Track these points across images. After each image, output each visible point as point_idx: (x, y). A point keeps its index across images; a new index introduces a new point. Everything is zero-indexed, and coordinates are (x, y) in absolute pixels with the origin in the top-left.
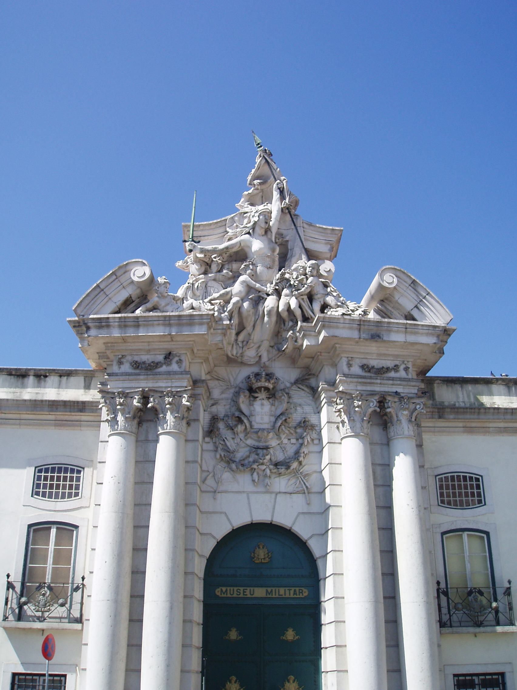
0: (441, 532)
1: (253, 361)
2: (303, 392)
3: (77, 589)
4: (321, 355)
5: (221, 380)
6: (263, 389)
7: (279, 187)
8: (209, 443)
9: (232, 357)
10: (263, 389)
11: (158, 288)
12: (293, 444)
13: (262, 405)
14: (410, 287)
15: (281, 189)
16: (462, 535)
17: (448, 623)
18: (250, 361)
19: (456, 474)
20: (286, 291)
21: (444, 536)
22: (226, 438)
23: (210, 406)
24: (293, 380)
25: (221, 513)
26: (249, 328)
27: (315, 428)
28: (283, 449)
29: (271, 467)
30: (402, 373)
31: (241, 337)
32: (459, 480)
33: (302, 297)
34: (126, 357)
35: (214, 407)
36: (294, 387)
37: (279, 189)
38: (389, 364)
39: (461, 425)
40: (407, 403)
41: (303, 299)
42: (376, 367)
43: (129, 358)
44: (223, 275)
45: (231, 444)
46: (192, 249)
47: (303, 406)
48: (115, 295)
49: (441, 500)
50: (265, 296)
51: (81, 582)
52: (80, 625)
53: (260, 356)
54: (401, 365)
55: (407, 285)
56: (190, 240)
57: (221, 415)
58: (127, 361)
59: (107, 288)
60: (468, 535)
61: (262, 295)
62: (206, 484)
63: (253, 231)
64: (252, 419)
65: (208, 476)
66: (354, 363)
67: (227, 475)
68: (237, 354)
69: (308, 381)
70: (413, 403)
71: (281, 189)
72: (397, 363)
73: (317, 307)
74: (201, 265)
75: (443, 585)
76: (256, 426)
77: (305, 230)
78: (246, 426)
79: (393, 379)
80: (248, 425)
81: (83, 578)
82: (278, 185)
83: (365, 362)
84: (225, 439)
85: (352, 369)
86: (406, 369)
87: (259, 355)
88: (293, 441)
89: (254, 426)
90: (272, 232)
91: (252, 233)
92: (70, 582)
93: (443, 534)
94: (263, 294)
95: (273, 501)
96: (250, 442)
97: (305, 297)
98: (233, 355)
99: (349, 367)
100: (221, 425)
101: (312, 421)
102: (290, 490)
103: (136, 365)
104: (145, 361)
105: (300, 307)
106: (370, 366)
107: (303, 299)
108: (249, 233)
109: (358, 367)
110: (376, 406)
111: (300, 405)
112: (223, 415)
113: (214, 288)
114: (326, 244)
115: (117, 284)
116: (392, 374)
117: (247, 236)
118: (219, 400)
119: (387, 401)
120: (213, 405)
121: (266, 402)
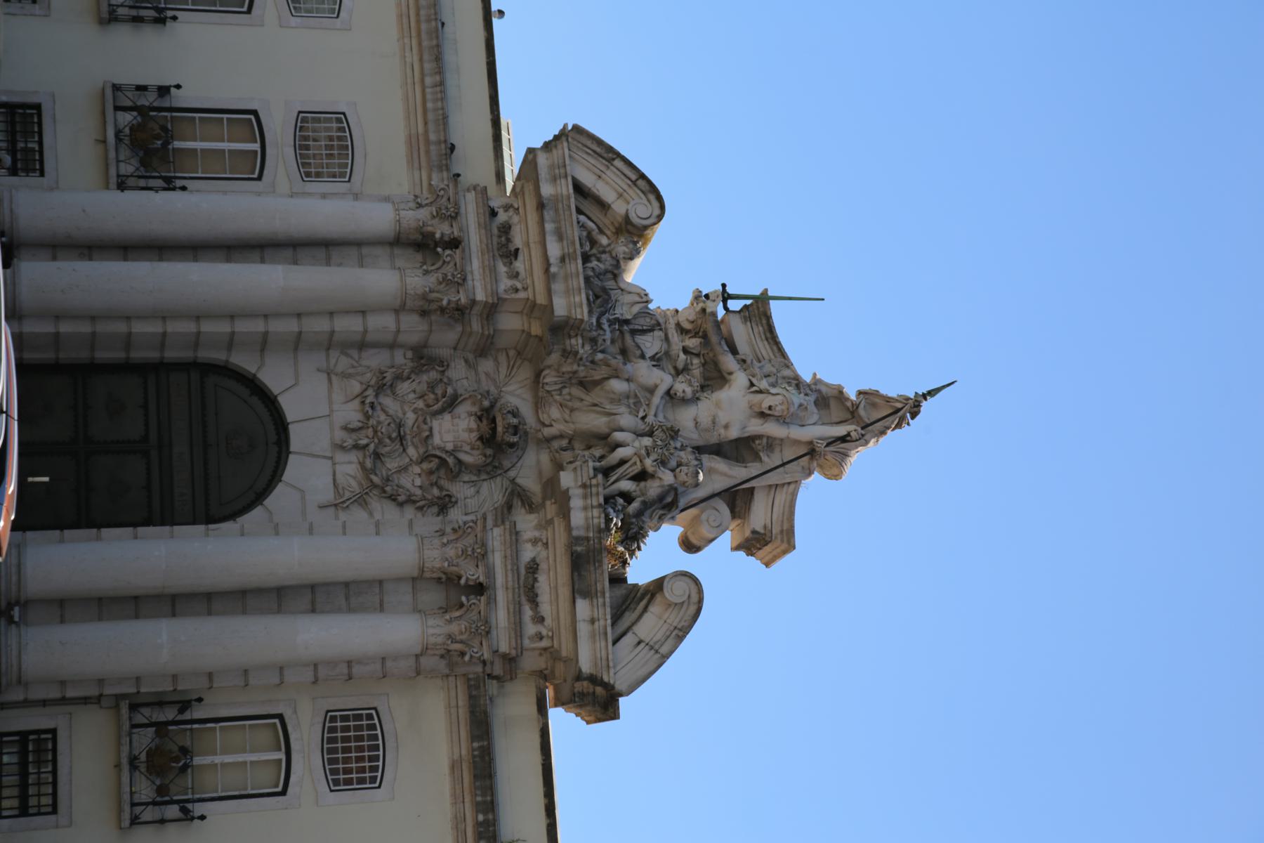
0: (284, 715)
1: (544, 418)
2: (500, 497)
3: (168, 180)
4: (552, 504)
5: (508, 368)
6: (493, 425)
7: (852, 434)
8: (405, 358)
9: (542, 378)
10: (493, 425)
11: (622, 242)
12: (413, 481)
13: (471, 431)
14: (672, 628)
15: (849, 438)
16: (280, 750)
17: (140, 719)
18: (543, 413)
19: (380, 742)
20: (647, 441)
21: (277, 721)
22: (414, 380)
23: (464, 357)
24: (519, 481)
25: (297, 379)
26: (589, 399)
27: (442, 513)
28: (403, 469)
29: (372, 447)
30: (531, 629)
31: (577, 391)
32: (371, 759)
33: (638, 463)
34: (517, 214)
35: (463, 364)
36: (506, 483)
37: (849, 435)
38: (546, 609)
39: (464, 752)
40: (479, 631)
41: (635, 463)
42: (537, 585)
43: (515, 219)
44: (678, 356)
45: (404, 387)
46: (711, 298)
47: (476, 497)
48: (607, 183)
49: (336, 716)
50: (641, 414)
51: (178, 186)
52: (115, 187)
53: (551, 426)
54: (545, 627)
55: (675, 624)
56: (726, 295)
57: (451, 373)
58: (510, 217)
59: (615, 170)
60: (280, 760)
61: (642, 410)
62: (339, 356)
63: (756, 392)
64: (447, 417)
65: (352, 357)
66: (539, 549)
67: (357, 388)
68: (547, 384)
69: (520, 503)
70: (481, 644)
71: (849, 438)
72: (548, 622)
73: (626, 485)
74: (693, 322)
75: (198, 713)
76: (435, 424)
77: (786, 486)
78: (433, 405)
79: (519, 612)
80: (436, 407)
81: (184, 188)
82: (855, 430)
83: (543, 566)
84: (411, 380)
85: (529, 546)
86: (540, 637)
87: (553, 423)
88: (418, 482)
89: (436, 420)
90: (762, 425)
91: (750, 391)
92: (177, 175)
93: (280, 717)
94: (645, 411)
95: (321, 453)
96: (410, 418)
97: (638, 468)
98: (544, 378)
99: (530, 540)
100: (434, 375)
101: (452, 509)
102: (338, 476)
103: (506, 229)
104: (511, 242)
105: (622, 462)
106: (536, 576)
107: (635, 463)
108: (752, 385)
109: (532, 556)
110: (467, 579)
111: (478, 492)
112: (450, 376)
113: (651, 340)
114: (765, 527)
115: (623, 184)
116: (528, 612)
117: (748, 383)
118: (476, 371)
119: (478, 597)
120: (466, 361)
121: (474, 435)
